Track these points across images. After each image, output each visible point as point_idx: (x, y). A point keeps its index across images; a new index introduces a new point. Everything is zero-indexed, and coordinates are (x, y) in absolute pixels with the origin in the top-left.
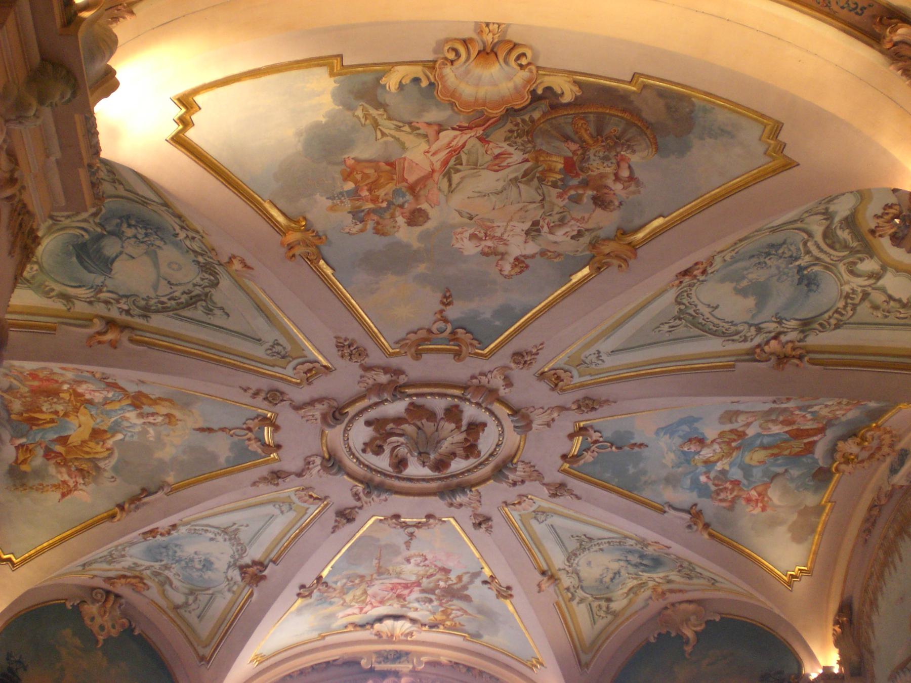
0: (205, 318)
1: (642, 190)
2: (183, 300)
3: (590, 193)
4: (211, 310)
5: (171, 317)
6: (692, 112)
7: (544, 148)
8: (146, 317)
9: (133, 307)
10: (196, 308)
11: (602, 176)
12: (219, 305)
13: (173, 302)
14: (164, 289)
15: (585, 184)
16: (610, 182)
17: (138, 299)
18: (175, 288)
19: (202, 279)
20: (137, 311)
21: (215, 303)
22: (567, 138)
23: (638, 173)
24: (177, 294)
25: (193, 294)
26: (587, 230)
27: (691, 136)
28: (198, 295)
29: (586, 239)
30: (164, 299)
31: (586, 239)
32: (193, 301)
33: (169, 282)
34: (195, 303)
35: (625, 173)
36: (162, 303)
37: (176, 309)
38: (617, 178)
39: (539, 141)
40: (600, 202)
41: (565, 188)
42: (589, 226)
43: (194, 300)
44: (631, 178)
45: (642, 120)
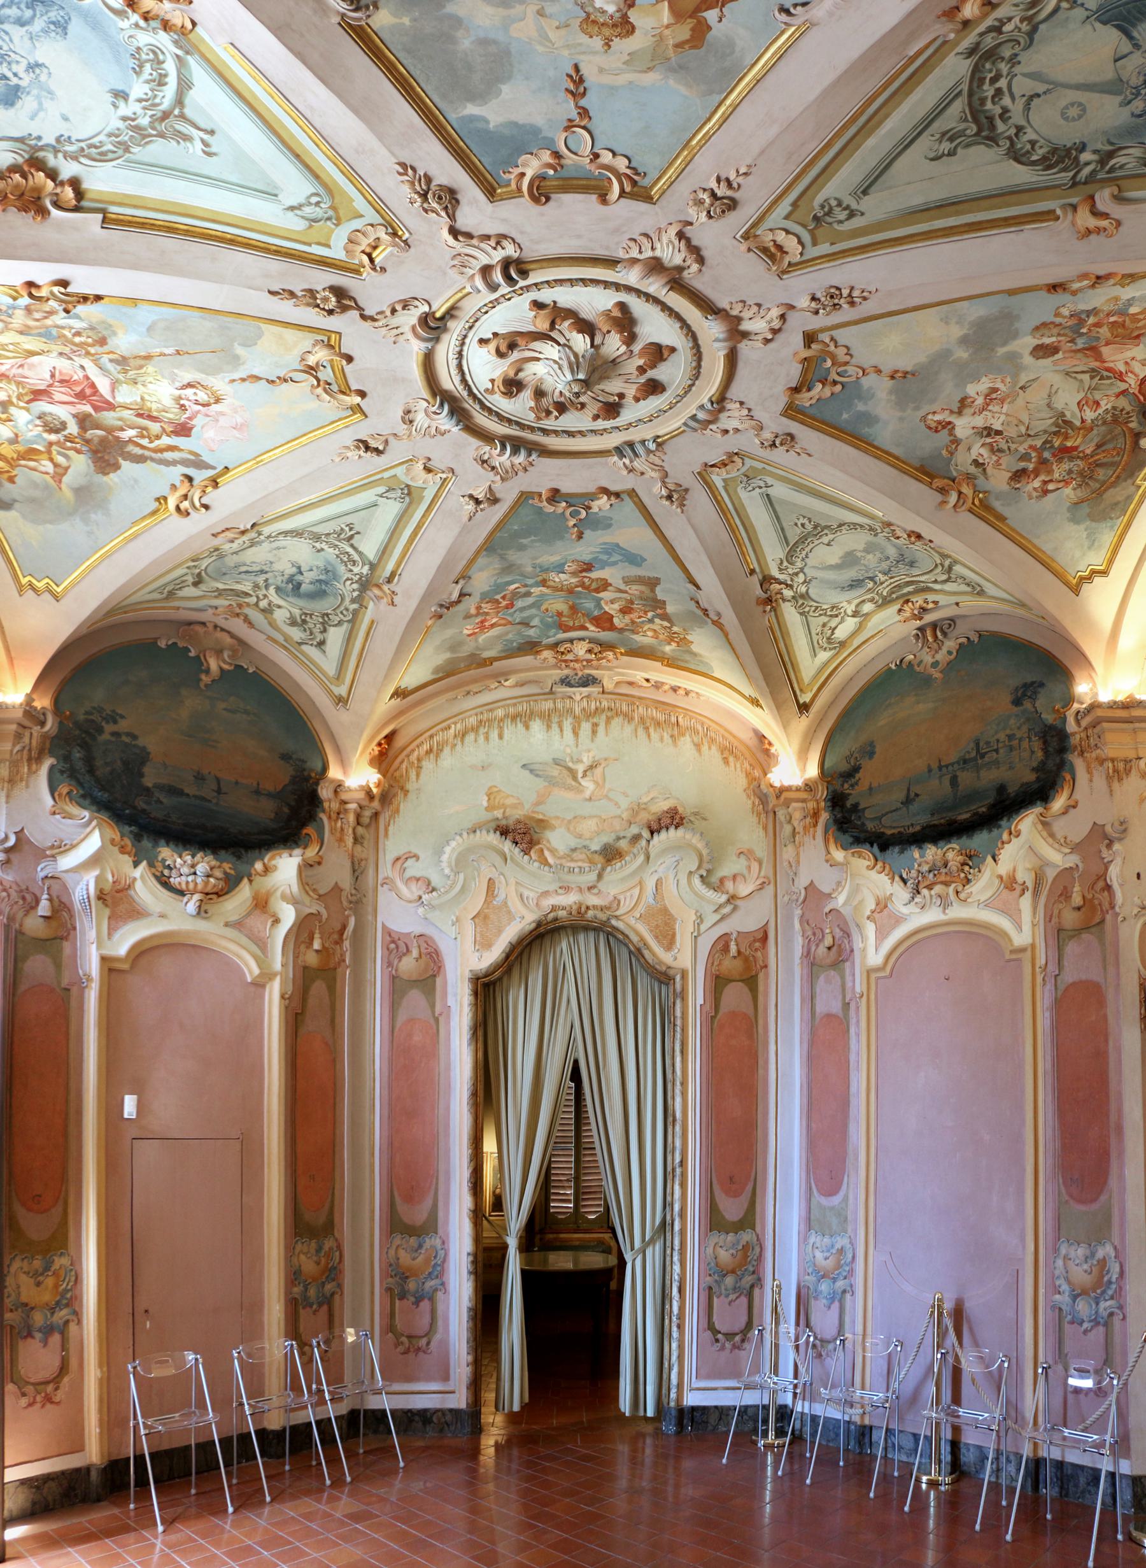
0: (939, 126)
1: (1033, 501)
2: (989, 105)
3: (1031, 466)
4: (951, 140)
5: (958, 83)
6: (1111, 518)
7: (1095, 432)
8: (971, 52)
9: (1002, 38)
10: (966, 120)
11: (1050, 472)
12: (959, 150)
13: (991, 93)
14: (1023, 86)
15: (1043, 462)
16: (1043, 477)
17: (1017, 49)
18: (1020, 103)
19: (1033, 143)
20: (989, 41)
21: (968, 146)
22: (1098, 446)
23: (1050, 496)
24: (1006, 101)
25: (999, 123)
26: (984, 470)
27: (1088, 523)
28: (992, 127)
29: (972, 470)
30: (1002, 83)
31: (972, 470)
32: (976, 112)
33: (1038, 95)
34: (976, 120)
35: (1051, 487)
36: (994, 80)
37: (971, 94)
38: (1045, 483)
39: (1103, 428)
40: (1019, 475)
41: (1040, 451)
42: (989, 470)
43: (985, 121)
44: (1046, 492)
45: (1105, 490)
